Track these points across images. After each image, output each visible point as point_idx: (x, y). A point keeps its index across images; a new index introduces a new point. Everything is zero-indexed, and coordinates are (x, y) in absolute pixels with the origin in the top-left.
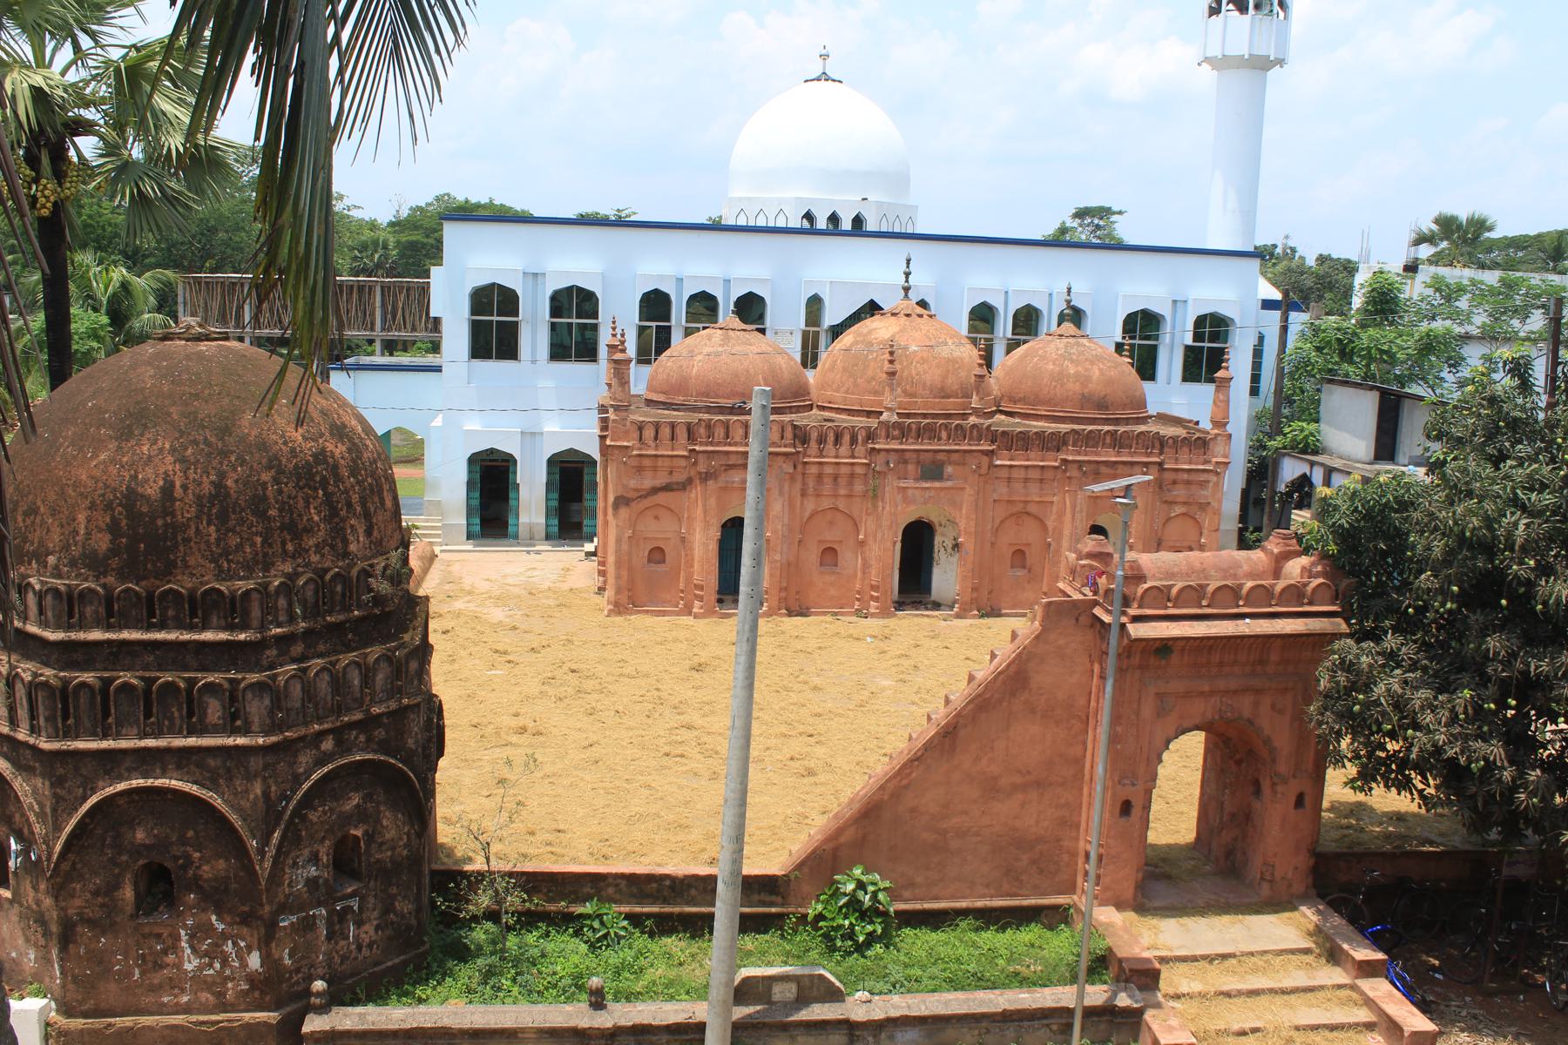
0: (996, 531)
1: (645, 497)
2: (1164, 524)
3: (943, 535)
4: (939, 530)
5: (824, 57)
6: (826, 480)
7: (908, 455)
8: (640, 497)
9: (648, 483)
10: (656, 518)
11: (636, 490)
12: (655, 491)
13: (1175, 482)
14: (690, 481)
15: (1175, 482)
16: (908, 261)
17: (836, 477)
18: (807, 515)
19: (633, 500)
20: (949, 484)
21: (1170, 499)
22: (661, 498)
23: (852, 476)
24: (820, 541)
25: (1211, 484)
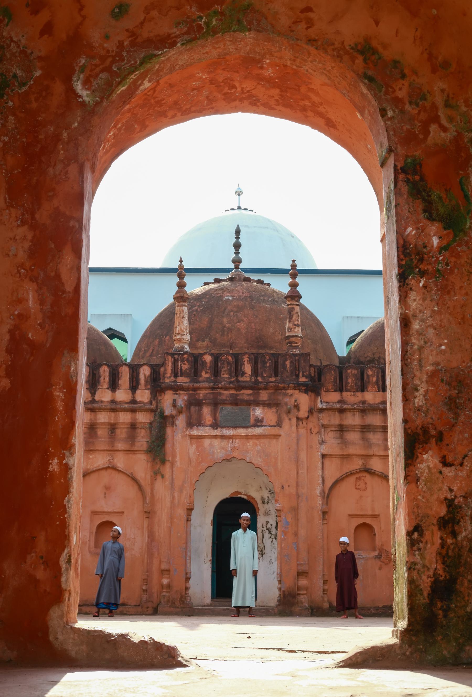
3: (267, 513)
4: (261, 508)
5: (239, 193)
6: (100, 432)
7: (202, 394)
16: (238, 232)
17: (113, 428)
20: (258, 431)
23: (133, 426)
24: (94, 513)
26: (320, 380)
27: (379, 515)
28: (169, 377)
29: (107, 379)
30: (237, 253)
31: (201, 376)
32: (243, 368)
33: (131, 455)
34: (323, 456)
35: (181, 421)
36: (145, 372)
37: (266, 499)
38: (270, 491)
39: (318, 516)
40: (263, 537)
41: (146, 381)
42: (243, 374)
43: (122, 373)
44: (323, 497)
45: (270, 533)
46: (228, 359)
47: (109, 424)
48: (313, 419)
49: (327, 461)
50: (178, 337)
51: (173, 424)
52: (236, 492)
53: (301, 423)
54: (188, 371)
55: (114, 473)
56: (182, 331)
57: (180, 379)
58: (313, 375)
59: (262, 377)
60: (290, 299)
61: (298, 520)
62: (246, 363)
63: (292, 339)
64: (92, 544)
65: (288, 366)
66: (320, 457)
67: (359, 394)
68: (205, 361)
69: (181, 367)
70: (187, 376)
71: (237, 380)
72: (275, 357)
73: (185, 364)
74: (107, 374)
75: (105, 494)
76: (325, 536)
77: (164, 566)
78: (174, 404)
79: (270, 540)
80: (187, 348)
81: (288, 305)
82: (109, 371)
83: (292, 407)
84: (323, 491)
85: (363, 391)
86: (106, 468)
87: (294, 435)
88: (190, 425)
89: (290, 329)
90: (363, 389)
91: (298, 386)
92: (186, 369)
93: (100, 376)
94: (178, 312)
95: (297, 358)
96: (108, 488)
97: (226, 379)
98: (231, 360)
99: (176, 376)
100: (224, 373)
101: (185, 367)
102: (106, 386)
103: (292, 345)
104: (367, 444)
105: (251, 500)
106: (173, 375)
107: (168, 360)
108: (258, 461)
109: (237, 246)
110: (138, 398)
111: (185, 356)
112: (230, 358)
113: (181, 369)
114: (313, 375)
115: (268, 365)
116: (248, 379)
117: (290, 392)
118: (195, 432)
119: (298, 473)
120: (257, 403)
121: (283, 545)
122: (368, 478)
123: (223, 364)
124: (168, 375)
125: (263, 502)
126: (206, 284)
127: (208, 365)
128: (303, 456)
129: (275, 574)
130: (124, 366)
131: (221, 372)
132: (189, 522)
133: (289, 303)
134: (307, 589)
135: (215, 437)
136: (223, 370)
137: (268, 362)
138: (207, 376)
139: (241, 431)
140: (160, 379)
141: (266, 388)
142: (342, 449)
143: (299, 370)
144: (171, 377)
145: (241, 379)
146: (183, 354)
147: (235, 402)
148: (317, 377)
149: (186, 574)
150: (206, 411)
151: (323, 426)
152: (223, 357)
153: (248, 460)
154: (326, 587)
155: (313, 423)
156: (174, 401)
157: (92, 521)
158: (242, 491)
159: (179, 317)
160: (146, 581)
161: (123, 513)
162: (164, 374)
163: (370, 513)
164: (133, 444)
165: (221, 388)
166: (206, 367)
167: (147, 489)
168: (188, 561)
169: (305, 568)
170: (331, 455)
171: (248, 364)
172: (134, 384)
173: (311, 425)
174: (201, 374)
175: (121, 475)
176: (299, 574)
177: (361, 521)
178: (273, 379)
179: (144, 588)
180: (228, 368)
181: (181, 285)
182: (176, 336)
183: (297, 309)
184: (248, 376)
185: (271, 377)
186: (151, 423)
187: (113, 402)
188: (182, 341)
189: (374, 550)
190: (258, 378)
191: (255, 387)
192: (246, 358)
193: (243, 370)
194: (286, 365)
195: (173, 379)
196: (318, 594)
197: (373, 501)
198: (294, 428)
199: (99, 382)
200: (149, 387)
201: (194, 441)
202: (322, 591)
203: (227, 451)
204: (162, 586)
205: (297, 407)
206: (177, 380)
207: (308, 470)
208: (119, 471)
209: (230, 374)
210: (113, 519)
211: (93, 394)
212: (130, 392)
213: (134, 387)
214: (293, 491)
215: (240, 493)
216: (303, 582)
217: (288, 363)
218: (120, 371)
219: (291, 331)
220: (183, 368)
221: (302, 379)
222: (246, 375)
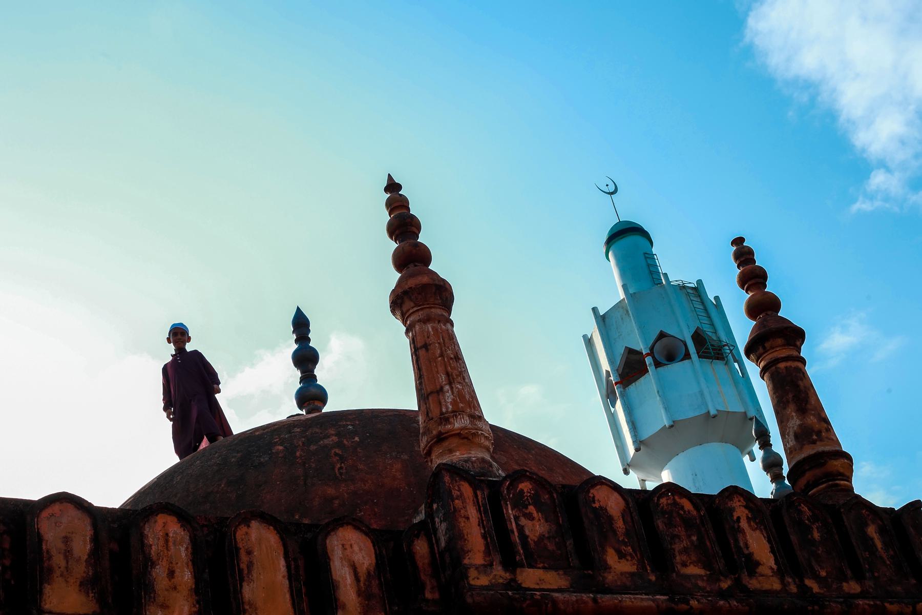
28: (485, 566)
29: (186, 576)
31: (607, 568)
32: (742, 544)
41: (364, 594)
42: (752, 565)
43: (249, 553)
46: (682, 508)
54: (551, 546)
57: (530, 577)
60: (780, 341)
62: (744, 524)
63: (835, 463)
68: (603, 509)
69: (521, 529)
70: (554, 564)
71: (739, 588)
73: (530, 517)
74: (183, 552)
82: (187, 538)
92: (541, 538)
94: (432, 339)
97: (700, 583)
98: (695, 513)
99: (510, 564)
100: (684, 558)
103: (837, 485)
106: (497, 558)
107: (461, 497)
113: (523, 537)
115: (816, 535)
127: (620, 524)
130: (254, 524)
131: (675, 557)
136: (678, 547)
137: (814, 527)
144: (491, 565)
152: (663, 501)
159: (442, 355)
166: (614, 532)
171: (754, 530)
174: (605, 561)
178: (853, 587)
180: (692, 542)
184: (769, 573)
185: (844, 578)
188: (476, 440)
190: (808, 582)
193: (746, 552)
194: (872, 539)
195: (499, 573)
206: (520, 579)
209: (707, 566)
217: (871, 530)
218: (240, 545)
219: (821, 440)
220: (527, 532)
222: (760, 569)
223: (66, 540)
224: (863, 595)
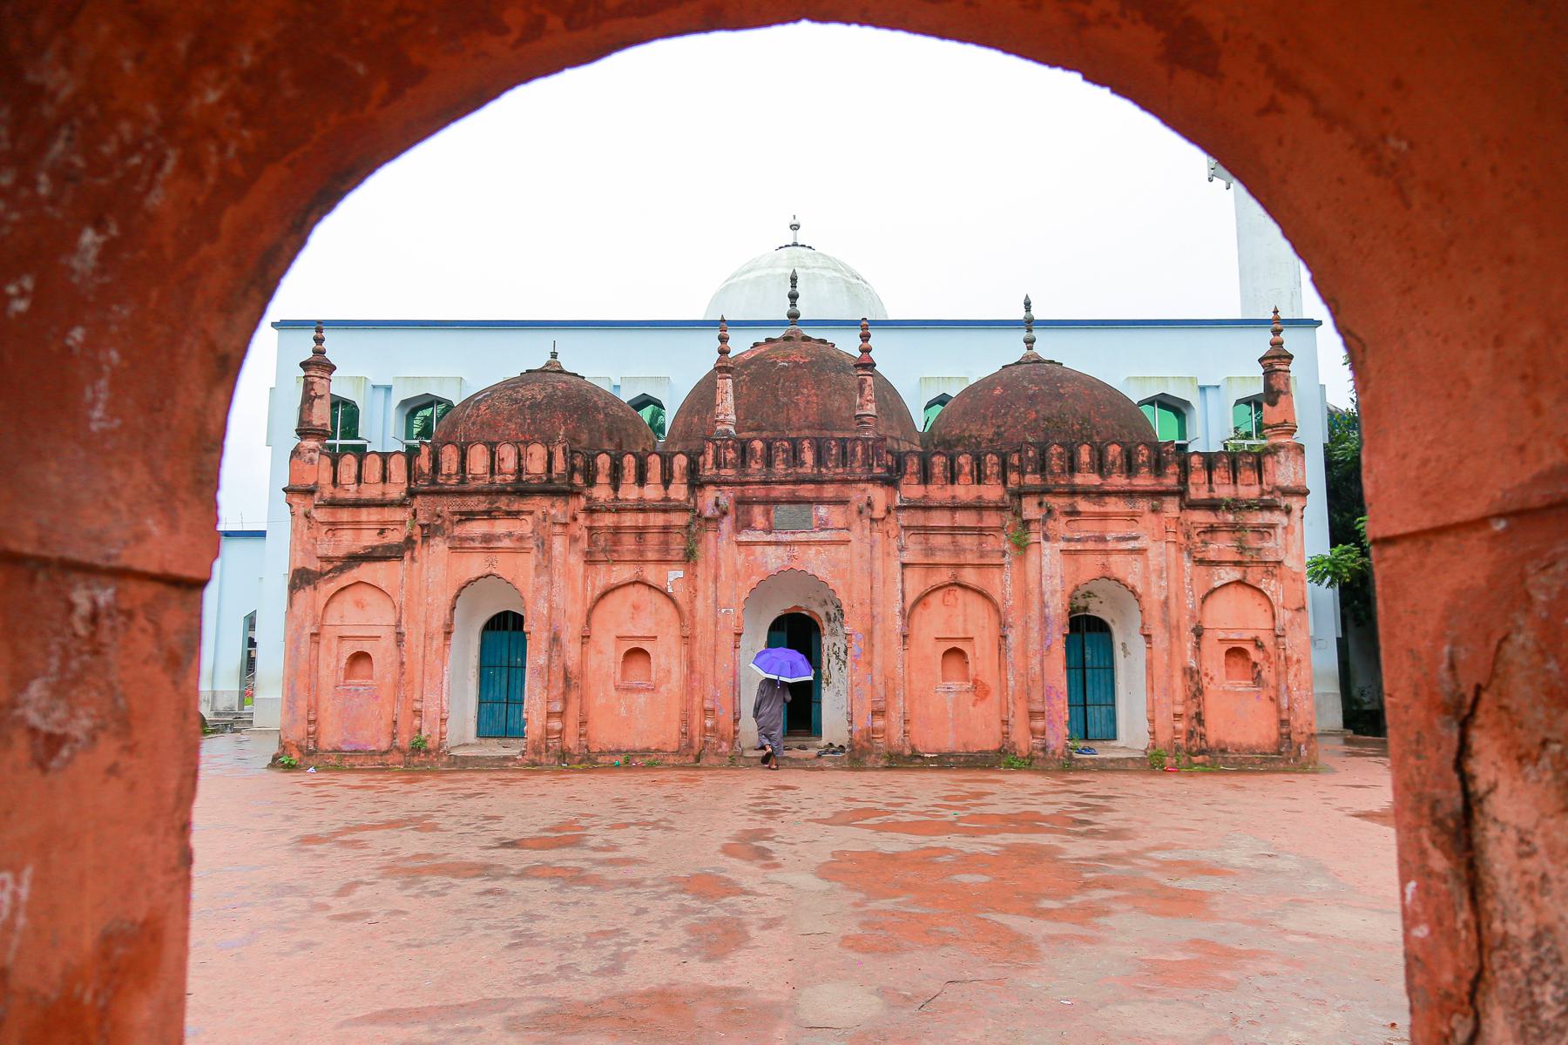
0: (907, 616)
1: (340, 570)
2: (1204, 600)
3: (834, 633)
4: (826, 628)
5: (795, 227)
8: (335, 569)
9: (349, 542)
10: (359, 604)
11: (328, 559)
12: (354, 559)
13: (1212, 529)
14: (409, 542)
15: (1212, 529)
16: (794, 280)
18: (597, 592)
19: (321, 575)
20: (823, 536)
21: (1212, 556)
22: (365, 572)
25: (1279, 531)
26: (898, 469)
27: (972, 638)
29: (633, 472)
30: (793, 305)
31: (750, 467)
33: (664, 567)
34: (904, 565)
35: (726, 525)
36: (680, 462)
37: (832, 616)
38: (837, 606)
39: (896, 639)
40: (829, 662)
42: (802, 464)
44: (904, 618)
45: (837, 657)
47: (637, 527)
48: (891, 520)
49: (908, 572)
50: (721, 417)
51: (717, 529)
52: (796, 607)
53: (875, 525)
55: (644, 590)
56: (726, 410)
57: (723, 472)
58: (890, 464)
59: (827, 467)
61: (873, 645)
64: (618, 676)
65: (859, 454)
66: (899, 567)
67: (949, 487)
70: (734, 466)
72: (842, 443)
73: (729, 452)
74: (633, 465)
75: (633, 614)
76: (906, 665)
77: (708, 705)
78: (717, 505)
79: (838, 667)
80: (732, 429)
81: (858, 376)
83: (865, 505)
84: (904, 609)
85: (952, 483)
86: (634, 583)
87: (867, 540)
88: (738, 530)
89: (861, 405)
90: (953, 478)
91: (873, 480)
93: (623, 468)
95: (870, 443)
96: (636, 607)
99: (718, 466)
101: (731, 455)
102: (632, 480)
104: (958, 550)
105: (812, 616)
106: (715, 466)
108: (822, 573)
109: (793, 297)
110: (673, 496)
111: (730, 442)
112: (786, 443)
113: (725, 459)
114: (890, 464)
116: (810, 471)
117: (862, 486)
118: (743, 538)
119: (871, 588)
120: (821, 502)
121: (854, 678)
122: (959, 592)
123: (778, 452)
124: (707, 467)
125: (829, 620)
126: (756, 345)
128: (878, 565)
129: (845, 710)
131: (775, 461)
132: (737, 650)
133: (860, 373)
134: (884, 731)
135: (769, 543)
136: (778, 458)
138: (758, 467)
139: (801, 537)
140: (699, 470)
141: (832, 482)
142: (926, 556)
143: (873, 459)
144: (712, 468)
145: (800, 471)
146: (728, 440)
147: (795, 501)
148: (895, 466)
149: (734, 714)
150: (757, 511)
151: (902, 527)
153: (810, 572)
154: (908, 728)
155: (892, 524)
156: (717, 498)
157: (617, 648)
158: (803, 605)
160: (686, 720)
161: (656, 637)
162: (704, 464)
163: (962, 636)
164: (667, 551)
165: (776, 482)
167: (685, 608)
168: (737, 698)
169: (882, 704)
170: (914, 564)
172: (667, 478)
173: (888, 527)
175: (652, 590)
176: (874, 713)
177: (951, 645)
178: (840, 470)
179: (683, 730)
181: (723, 352)
182: (717, 416)
183: (870, 380)
185: (837, 467)
186: (688, 527)
187: (641, 499)
189: (967, 679)
191: (818, 481)
192: (806, 444)
196: (897, 736)
197: (965, 620)
198: (867, 532)
199: (623, 476)
200: (685, 481)
201: (743, 549)
202: (902, 732)
203: (783, 561)
204: (705, 727)
205: (869, 505)
207: (884, 582)
208: (650, 587)
210: (645, 646)
211: (616, 489)
212: (662, 487)
213: (666, 481)
214: (867, 610)
215: (801, 608)
216: (879, 723)
217: (859, 449)
221: (877, 471)
223: (603, 464)
224: (843, 473)
